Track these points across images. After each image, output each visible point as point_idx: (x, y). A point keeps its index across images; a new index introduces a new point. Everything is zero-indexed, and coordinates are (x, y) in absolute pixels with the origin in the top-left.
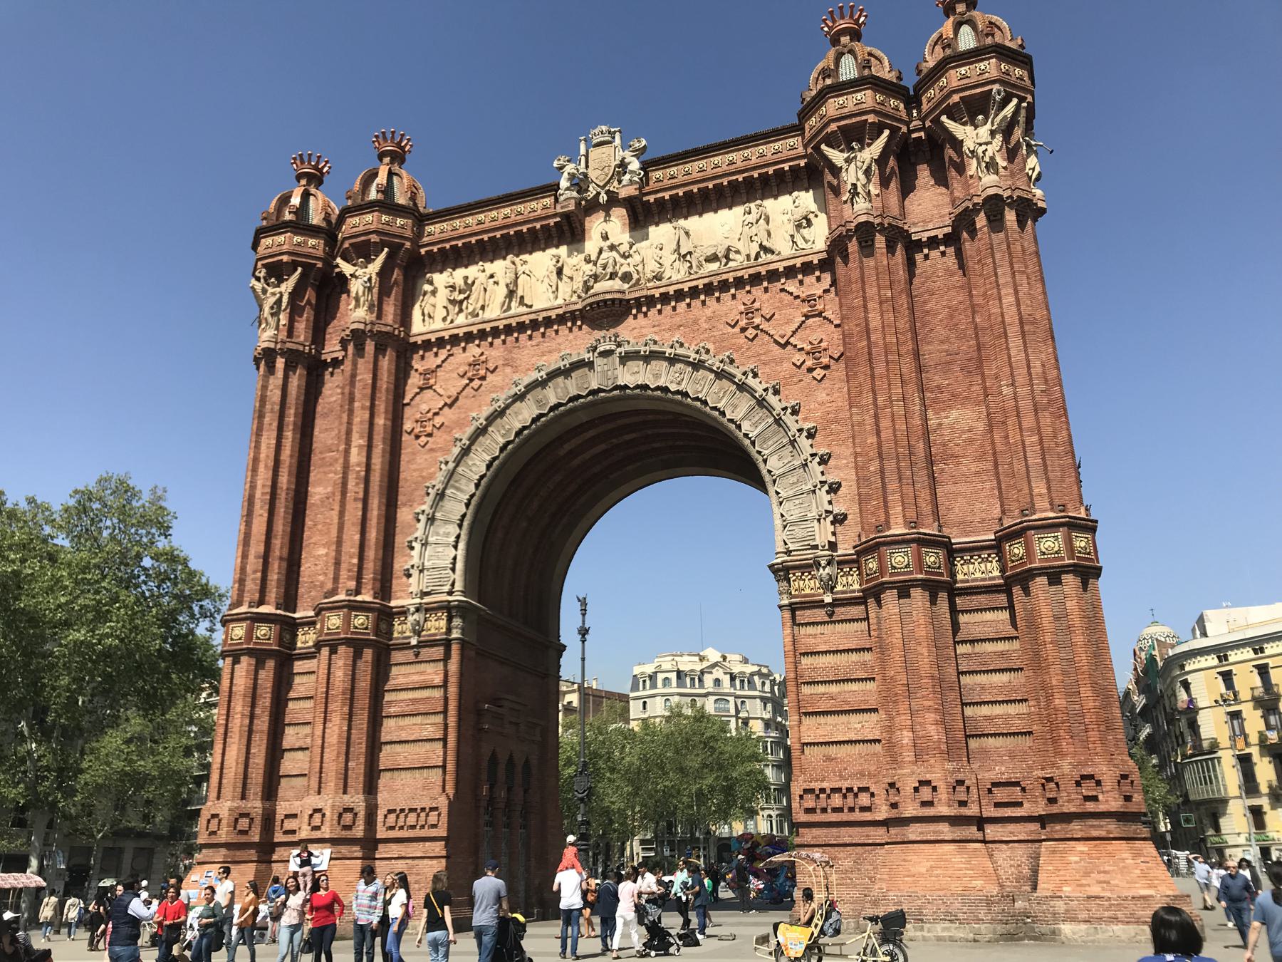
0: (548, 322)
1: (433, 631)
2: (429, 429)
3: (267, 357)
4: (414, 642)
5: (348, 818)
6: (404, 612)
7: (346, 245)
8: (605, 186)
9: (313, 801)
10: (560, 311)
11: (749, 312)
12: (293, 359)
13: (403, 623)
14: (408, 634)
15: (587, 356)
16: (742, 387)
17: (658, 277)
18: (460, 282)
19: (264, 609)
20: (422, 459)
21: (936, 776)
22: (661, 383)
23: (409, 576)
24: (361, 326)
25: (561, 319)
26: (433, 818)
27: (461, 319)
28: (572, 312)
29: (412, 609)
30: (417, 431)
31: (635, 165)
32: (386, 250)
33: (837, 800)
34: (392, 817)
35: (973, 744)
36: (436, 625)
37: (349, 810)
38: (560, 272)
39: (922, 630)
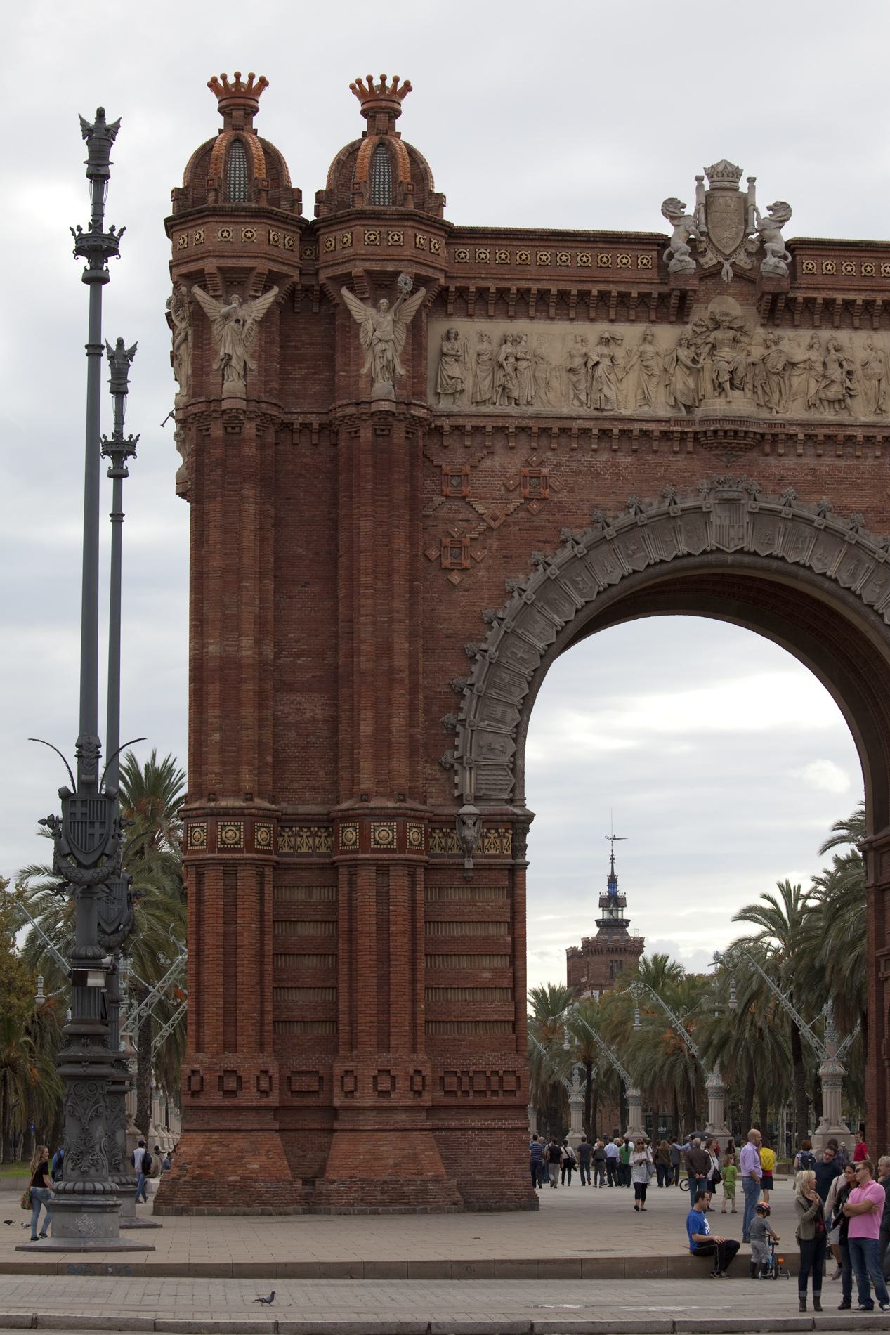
0: (645, 433)
1: (492, 851)
2: (467, 563)
4: (469, 864)
5: (418, 1079)
7: (358, 269)
8: (730, 255)
10: (663, 427)
12: (265, 420)
13: (448, 837)
14: (456, 851)
22: (804, 558)
23: (449, 770)
24: (393, 408)
25: (665, 435)
26: (510, 1083)
28: (682, 433)
29: (470, 822)
30: (447, 563)
32: (423, 291)
34: (451, 1081)
36: (495, 845)
37: (418, 1072)
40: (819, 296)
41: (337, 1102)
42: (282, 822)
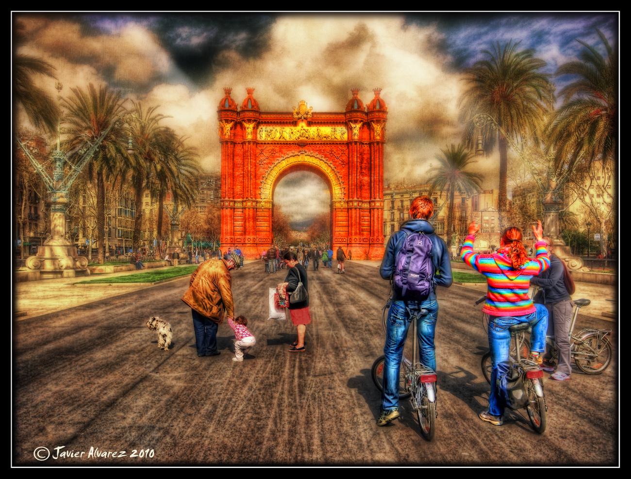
3: (227, 142)
6: (260, 202)
9: (247, 237)
11: (332, 151)
15: (299, 154)
16: (330, 166)
17: (314, 139)
18: (269, 130)
19: (231, 199)
20: (261, 170)
21: (357, 237)
22: (314, 162)
27: (269, 139)
31: (310, 113)
33: (340, 240)
35: (362, 232)
38: (292, 133)
39: (358, 215)
40: (317, 121)
41: (243, 242)
42: (235, 202)
